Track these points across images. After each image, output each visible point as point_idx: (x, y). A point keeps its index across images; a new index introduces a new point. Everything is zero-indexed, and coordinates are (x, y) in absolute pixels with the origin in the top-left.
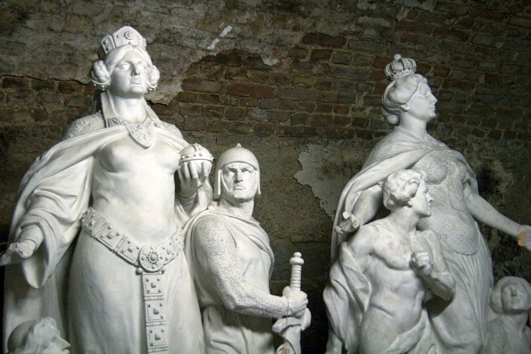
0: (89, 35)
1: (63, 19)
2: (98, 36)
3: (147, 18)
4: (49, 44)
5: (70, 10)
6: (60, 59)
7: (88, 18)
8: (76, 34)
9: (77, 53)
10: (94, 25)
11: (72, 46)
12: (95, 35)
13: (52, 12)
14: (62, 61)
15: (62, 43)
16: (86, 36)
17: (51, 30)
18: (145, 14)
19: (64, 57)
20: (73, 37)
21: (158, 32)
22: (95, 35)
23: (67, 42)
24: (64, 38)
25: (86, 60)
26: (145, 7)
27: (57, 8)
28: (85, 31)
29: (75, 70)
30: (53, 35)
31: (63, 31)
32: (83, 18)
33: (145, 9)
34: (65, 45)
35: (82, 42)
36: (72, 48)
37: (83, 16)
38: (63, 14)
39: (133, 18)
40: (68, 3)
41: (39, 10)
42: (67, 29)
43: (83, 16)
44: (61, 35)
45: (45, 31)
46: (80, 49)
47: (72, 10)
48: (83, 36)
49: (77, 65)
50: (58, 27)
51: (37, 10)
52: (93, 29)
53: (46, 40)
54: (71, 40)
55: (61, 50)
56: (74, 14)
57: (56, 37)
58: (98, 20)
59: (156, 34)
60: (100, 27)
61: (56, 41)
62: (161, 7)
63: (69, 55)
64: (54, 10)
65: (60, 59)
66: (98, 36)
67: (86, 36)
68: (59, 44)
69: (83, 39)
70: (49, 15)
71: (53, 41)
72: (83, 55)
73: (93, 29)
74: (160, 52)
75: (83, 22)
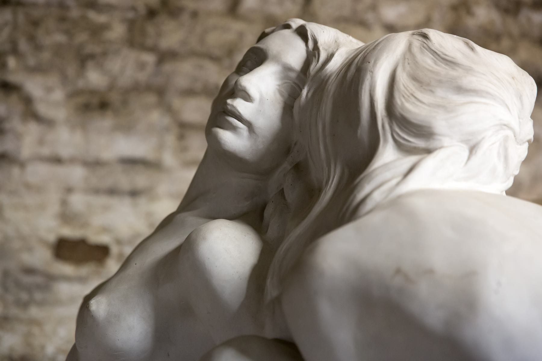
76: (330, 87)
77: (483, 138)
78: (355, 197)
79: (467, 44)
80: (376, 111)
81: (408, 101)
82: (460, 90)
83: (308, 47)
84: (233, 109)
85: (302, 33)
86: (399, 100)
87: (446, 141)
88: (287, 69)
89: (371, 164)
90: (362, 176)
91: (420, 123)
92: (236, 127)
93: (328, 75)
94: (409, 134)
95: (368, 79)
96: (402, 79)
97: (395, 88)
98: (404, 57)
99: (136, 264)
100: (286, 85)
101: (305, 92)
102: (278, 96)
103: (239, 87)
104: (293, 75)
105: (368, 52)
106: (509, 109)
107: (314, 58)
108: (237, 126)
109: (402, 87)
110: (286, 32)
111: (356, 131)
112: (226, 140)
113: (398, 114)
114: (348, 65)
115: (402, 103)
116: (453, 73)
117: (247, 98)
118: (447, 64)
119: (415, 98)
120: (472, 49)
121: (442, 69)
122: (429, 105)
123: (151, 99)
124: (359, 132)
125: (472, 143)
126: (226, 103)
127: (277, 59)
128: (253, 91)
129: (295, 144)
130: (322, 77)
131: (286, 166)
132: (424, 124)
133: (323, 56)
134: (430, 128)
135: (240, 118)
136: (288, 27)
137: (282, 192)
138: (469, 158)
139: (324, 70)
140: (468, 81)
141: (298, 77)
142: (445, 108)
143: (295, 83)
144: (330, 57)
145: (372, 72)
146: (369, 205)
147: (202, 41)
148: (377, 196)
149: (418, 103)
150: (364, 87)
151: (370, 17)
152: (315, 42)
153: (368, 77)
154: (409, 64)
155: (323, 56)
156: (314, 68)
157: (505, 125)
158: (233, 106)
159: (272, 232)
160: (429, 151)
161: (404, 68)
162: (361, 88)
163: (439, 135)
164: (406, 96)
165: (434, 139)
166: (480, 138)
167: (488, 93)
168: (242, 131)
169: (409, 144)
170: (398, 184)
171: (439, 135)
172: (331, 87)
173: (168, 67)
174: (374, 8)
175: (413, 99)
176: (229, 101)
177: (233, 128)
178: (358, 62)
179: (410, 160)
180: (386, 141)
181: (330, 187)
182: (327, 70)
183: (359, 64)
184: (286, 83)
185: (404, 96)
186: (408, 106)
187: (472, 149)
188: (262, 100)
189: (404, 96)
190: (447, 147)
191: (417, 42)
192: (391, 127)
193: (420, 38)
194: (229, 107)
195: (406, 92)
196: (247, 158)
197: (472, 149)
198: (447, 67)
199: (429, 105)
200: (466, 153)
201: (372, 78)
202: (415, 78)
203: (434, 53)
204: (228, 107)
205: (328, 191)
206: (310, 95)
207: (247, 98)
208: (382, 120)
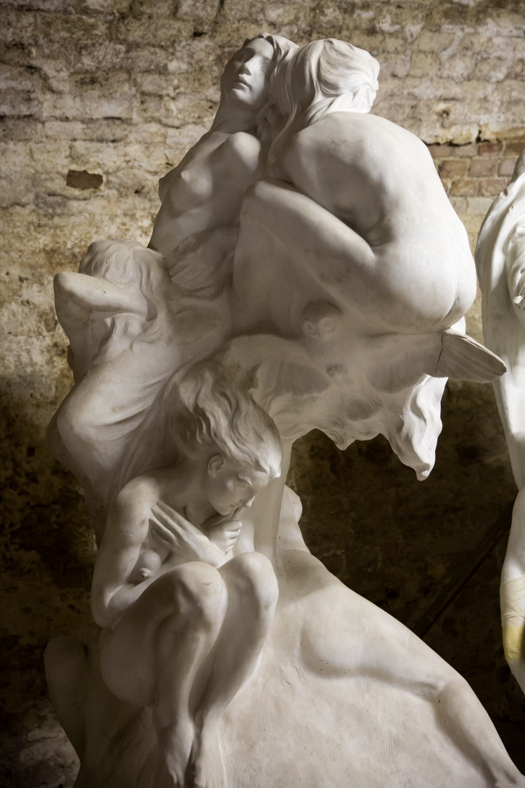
0: (435, 78)
1: (408, 58)
2: (444, 78)
3: (498, 46)
4: (392, 95)
5: (415, 47)
6: (403, 114)
7: (434, 55)
8: (421, 78)
9: (421, 104)
10: (440, 64)
11: (416, 94)
12: (441, 77)
13: (397, 52)
14: (405, 116)
15: (406, 92)
16: (432, 80)
17: (394, 76)
18: (497, 41)
19: (408, 110)
20: (417, 82)
21: (510, 64)
22: (441, 77)
23: (411, 90)
24: (408, 85)
25: (431, 112)
26: (498, 32)
27: (402, 46)
28: (431, 73)
29: (419, 127)
30: (396, 82)
31: (407, 76)
32: (430, 56)
33: (498, 34)
34: (409, 94)
35: (427, 88)
36: (415, 98)
37: (429, 53)
38: (408, 52)
39: (483, 49)
40: (415, 36)
41: (384, 51)
42: (412, 72)
43: (429, 53)
44: (404, 82)
45: (389, 78)
46: (425, 98)
47: (418, 46)
48: (428, 80)
49: (420, 120)
50: (401, 71)
51: (381, 50)
52: (439, 69)
53: (389, 90)
54: (415, 87)
55: (404, 102)
56: (420, 51)
57: (399, 85)
58: (445, 55)
59: (508, 68)
60: (447, 65)
61: (399, 90)
62: (516, 28)
63: (412, 107)
64: (399, 48)
65: (403, 114)
66: (444, 78)
67: (432, 80)
68: (402, 93)
69: (428, 83)
70: (393, 56)
71: (396, 90)
72: (427, 106)
73: (439, 69)
74: (511, 92)
75: (429, 60)
76: (289, 67)
77: (359, 89)
79: (349, 46)
81: (327, 73)
82: (349, 68)
85: (270, 40)
86: (323, 73)
87: (344, 91)
88: (265, 59)
89: (312, 103)
90: (309, 107)
93: (287, 62)
96: (323, 63)
97: (320, 67)
98: (323, 52)
101: (276, 70)
102: (262, 72)
104: (268, 62)
105: (306, 50)
106: (369, 76)
107: (279, 54)
109: (323, 67)
110: (261, 39)
114: (297, 56)
115: (324, 75)
116: (345, 60)
117: (249, 73)
118: (342, 56)
119: (330, 72)
120: (352, 48)
121: (340, 58)
122: (336, 75)
123: (124, 76)
124: (305, 88)
125: (354, 92)
126: (239, 77)
127: (260, 54)
128: (251, 70)
129: (271, 95)
133: (283, 52)
135: (245, 83)
136: (261, 37)
137: (265, 119)
138: (353, 98)
140: (352, 64)
141: (271, 63)
142: (343, 76)
143: (270, 66)
144: (287, 53)
145: (309, 60)
146: (315, 119)
147: (155, 36)
148: (318, 115)
149: (331, 74)
150: (306, 67)
152: (278, 45)
153: (308, 63)
154: (325, 56)
155: (283, 52)
156: (279, 58)
157: (367, 83)
158: (242, 78)
159: (264, 137)
160: (337, 96)
161: (323, 59)
164: (326, 71)
166: (357, 89)
167: (360, 69)
170: (326, 110)
171: (341, 88)
172: (290, 68)
173: (133, 54)
175: (329, 73)
176: (240, 75)
177: (242, 89)
178: (302, 55)
179: (330, 100)
181: (293, 113)
183: (302, 55)
185: (325, 71)
186: (327, 75)
187: (355, 94)
188: (255, 74)
189: (325, 71)
190: (345, 93)
191: (328, 45)
192: (320, 85)
193: (329, 43)
194: (240, 78)
195: (325, 69)
197: (355, 94)
198: (342, 57)
199: (336, 75)
200: (352, 96)
202: (329, 63)
203: (336, 51)
206: (278, 71)
207: (249, 73)
208: (316, 82)
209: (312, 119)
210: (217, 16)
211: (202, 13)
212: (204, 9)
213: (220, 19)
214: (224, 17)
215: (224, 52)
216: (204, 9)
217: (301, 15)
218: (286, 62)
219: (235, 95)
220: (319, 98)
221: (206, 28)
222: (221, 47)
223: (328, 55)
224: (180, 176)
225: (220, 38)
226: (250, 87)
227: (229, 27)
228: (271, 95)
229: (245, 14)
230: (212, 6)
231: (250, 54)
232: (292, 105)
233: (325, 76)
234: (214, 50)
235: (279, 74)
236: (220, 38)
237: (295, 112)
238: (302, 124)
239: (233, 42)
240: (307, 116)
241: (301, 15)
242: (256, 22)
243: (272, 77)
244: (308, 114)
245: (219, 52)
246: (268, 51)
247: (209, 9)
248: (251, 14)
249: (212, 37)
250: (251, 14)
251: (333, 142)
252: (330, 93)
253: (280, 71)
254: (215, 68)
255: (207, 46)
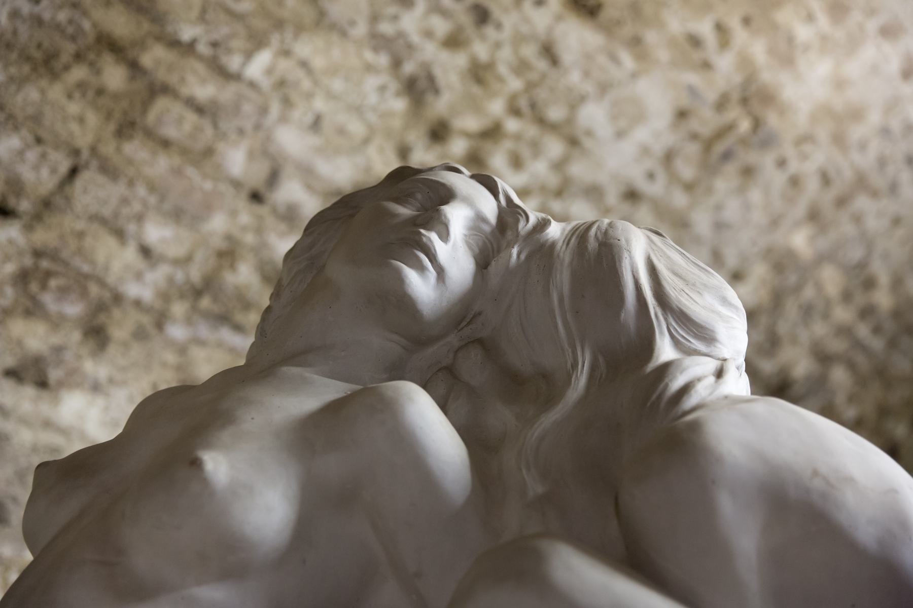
76: (561, 254)
78: (667, 385)
80: (645, 296)
81: (681, 296)
83: (500, 202)
84: (429, 243)
88: (480, 218)
89: (655, 354)
91: (703, 324)
92: (426, 267)
94: (688, 334)
95: (626, 258)
99: (253, 419)
100: (475, 237)
101: (515, 251)
103: (443, 217)
104: (487, 229)
108: (427, 266)
111: (618, 314)
112: (412, 280)
113: (674, 306)
117: (445, 236)
124: (623, 315)
127: (468, 201)
130: (541, 241)
131: (453, 340)
132: (707, 326)
133: (533, 219)
134: (713, 331)
135: (432, 258)
139: (544, 233)
141: (493, 232)
143: (487, 238)
150: (623, 265)
151: (132, 228)
156: (524, 227)
162: (621, 266)
163: (721, 343)
165: (715, 346)
168: (430, 275)
169: (689, 344)
171: (721, 343)
172: (565, 256)
174: (140, 218)
176: (422, 231)
177: (421, 268)
178: (596, 234)
180: (661, 333)
182: (548, 234)
184: (476, 235)
192: (666, 319)
194: (424, 239)
196: (425, 313)
201: (631, 258)
202: (676, 274)
204: (422, 239)
205: (580, 375)
206: (523, 257)
208: (654, 308)
209: (685, 398)
210: (53, 194)
211: (27, 174)
212: (36, 168)
213: (59, 201)
214: (68, 199)
215: (36, 267)
216: (36, 168)
217: (199, 256)
218: (547, 240)
219: (400, 279)
220: (665, 351)
221: (24, 206)
222: (38, 254)
223: (669, 257)
224: (196, 464)
225: (43, 237)
226: (440, 272)
227: (71, 223)
228: (480, 314)
229: (107, 212)
230: (54, 171)
231: (447, 195)
232: (575, 348)
233: (680, 301)
234: (20, 254)
235: (525, 267)
236: (43, 237)
237: (585, 368)
238: (649, 404)
239: (65, 254)
240: (662, 386)
241: (199, 256)
242: (120, 234)
243: (494, 267)
244: (666, 380)
245: (28, 261)
246: (489, 207)
247: (45, 173)
248: (116, 215)
249: (29, 228)
250: (116, 215)
251: (815, 473)
252: (694, 347)
253: (529, 257)
254: (9, 291)
255: (11, 242)
